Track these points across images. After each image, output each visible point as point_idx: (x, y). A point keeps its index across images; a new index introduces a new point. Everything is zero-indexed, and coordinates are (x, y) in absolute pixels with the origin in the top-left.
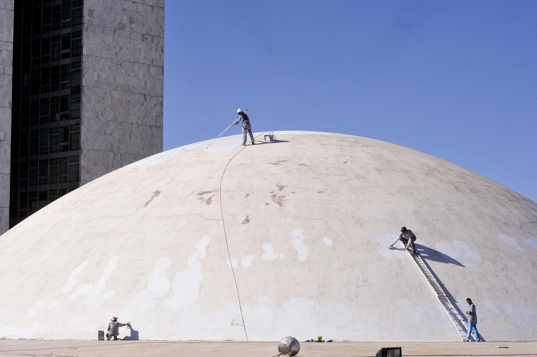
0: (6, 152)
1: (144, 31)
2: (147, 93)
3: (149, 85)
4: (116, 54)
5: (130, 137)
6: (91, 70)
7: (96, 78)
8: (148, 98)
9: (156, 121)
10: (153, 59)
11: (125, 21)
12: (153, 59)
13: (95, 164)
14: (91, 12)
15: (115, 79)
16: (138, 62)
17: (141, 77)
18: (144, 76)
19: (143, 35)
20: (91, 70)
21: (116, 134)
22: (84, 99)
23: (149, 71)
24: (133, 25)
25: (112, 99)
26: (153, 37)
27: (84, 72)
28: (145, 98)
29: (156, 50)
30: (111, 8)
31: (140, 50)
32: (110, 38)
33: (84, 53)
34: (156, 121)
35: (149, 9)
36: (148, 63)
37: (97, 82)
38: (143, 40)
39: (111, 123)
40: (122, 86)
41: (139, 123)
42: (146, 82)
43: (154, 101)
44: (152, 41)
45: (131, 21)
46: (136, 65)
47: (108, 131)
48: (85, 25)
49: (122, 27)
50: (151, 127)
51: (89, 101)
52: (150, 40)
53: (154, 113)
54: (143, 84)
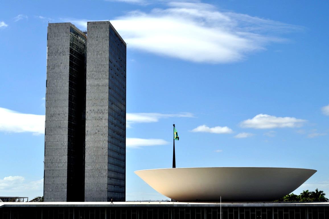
0: (66, 165)
1: (102, 133)
2: (103, 147)
3: (103, 146)
4: (94, 140)
5: (98, 158)
6: (88, 144)
7: (89, 146)
8: (103, 149)
9: (106, 154)
10: (105, 139)
11: (97, 131)
12: (105, 139)
13: (89, 165)
14: (87, 131)
15: (94, 145)
16: (101, 141)
17: (101, 144)
18: (102, 143)
19: (102, 134)
20: (88, 144)
21: (94, 158)
22: (86, 151)
23: (104, 142)
24: (99, 132)
25: (93, 150)
26: (105, 134)
27: (86, 145)
28: (103, 149)
29: (106, 137)
30: (93, 129)
31: (101, 138)
32: (93, 136)
33: (86, 141)
34: (106, 154)
35: (104, 128)
36: (103, 140)
37: (89, 147)
38: (102, 135)
39: (93, 156)
40: (96, 147)
41: (101, 155)
42: (103, 145)
43: (105, 149)
44: (105, 135)
45: (99, 131)
46: (100, 142)
47: (92, 158)
48: (86, 135)
49: (96, 133)
50: (104, 155)
51: (87, 151)
52: (104, 135)
53: (105, 152)
54: (102, 146)
